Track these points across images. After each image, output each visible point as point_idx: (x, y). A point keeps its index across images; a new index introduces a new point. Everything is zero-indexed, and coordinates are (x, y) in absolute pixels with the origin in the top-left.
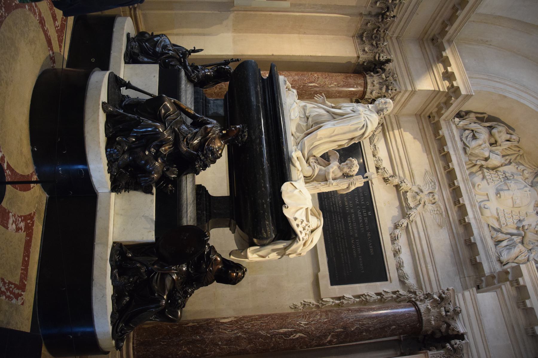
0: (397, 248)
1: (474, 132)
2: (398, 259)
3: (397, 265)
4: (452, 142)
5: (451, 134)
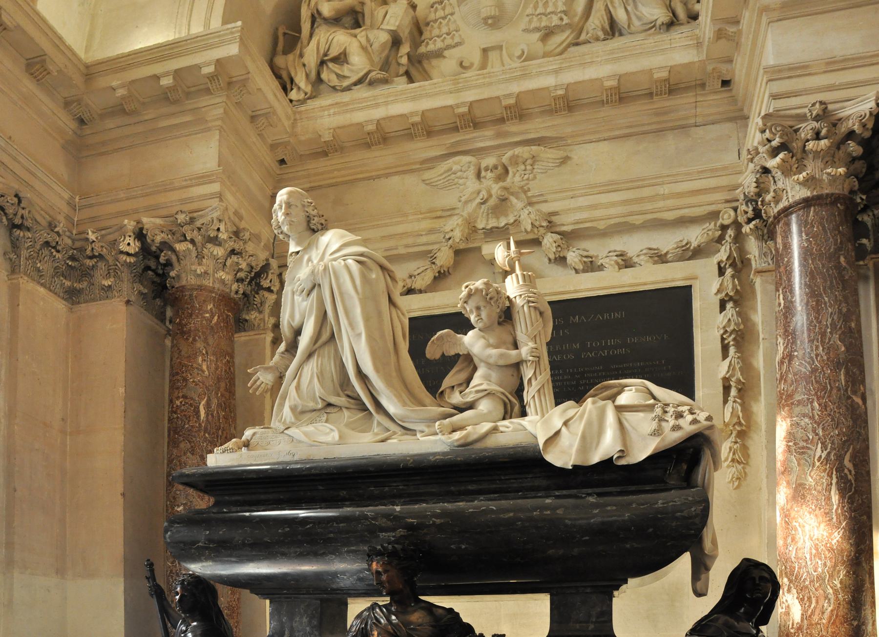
0: (615, 258)
1: (326, 58)
2: (642, 257)
3: (655, 263)
4: (352, 110)
5: (332, 111)
